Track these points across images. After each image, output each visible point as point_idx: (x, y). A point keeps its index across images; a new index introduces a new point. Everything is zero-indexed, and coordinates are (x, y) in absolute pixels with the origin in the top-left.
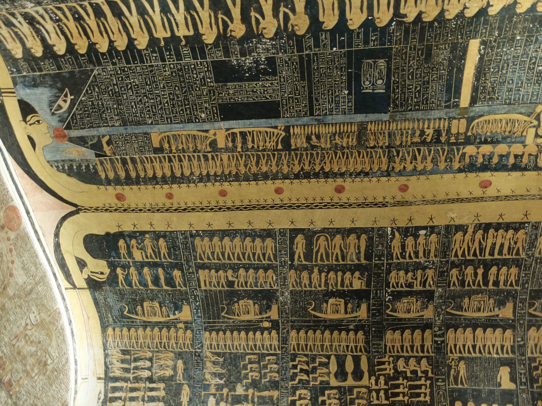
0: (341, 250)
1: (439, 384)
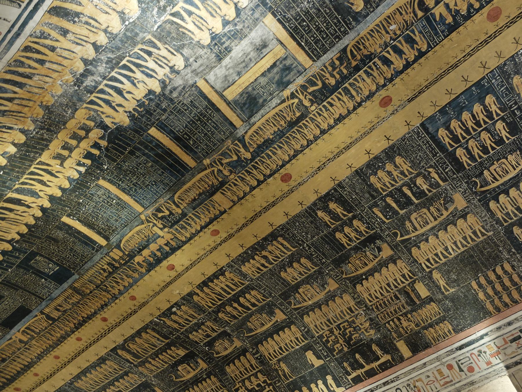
0: (148, 344)
1: (278, 385)
